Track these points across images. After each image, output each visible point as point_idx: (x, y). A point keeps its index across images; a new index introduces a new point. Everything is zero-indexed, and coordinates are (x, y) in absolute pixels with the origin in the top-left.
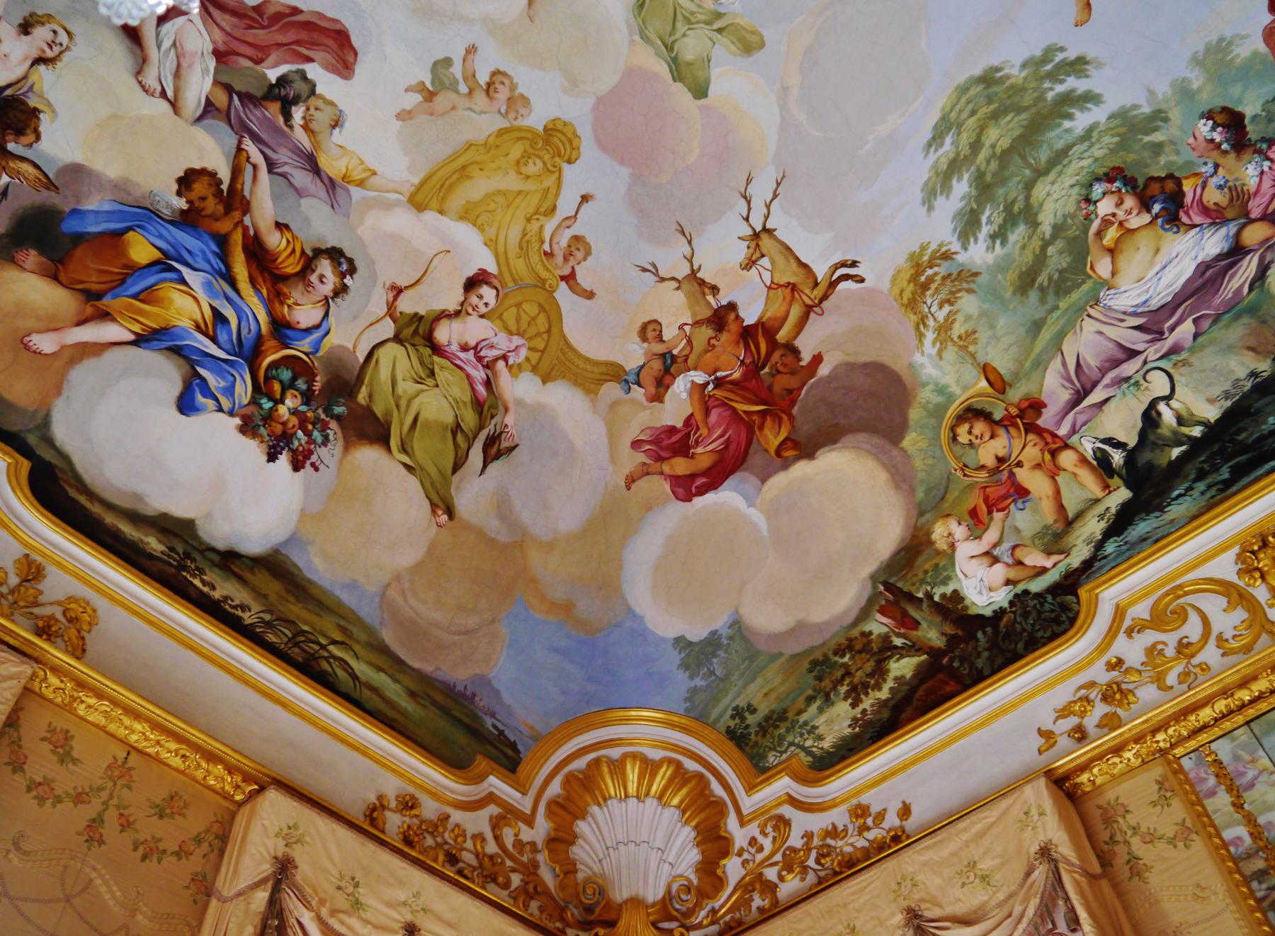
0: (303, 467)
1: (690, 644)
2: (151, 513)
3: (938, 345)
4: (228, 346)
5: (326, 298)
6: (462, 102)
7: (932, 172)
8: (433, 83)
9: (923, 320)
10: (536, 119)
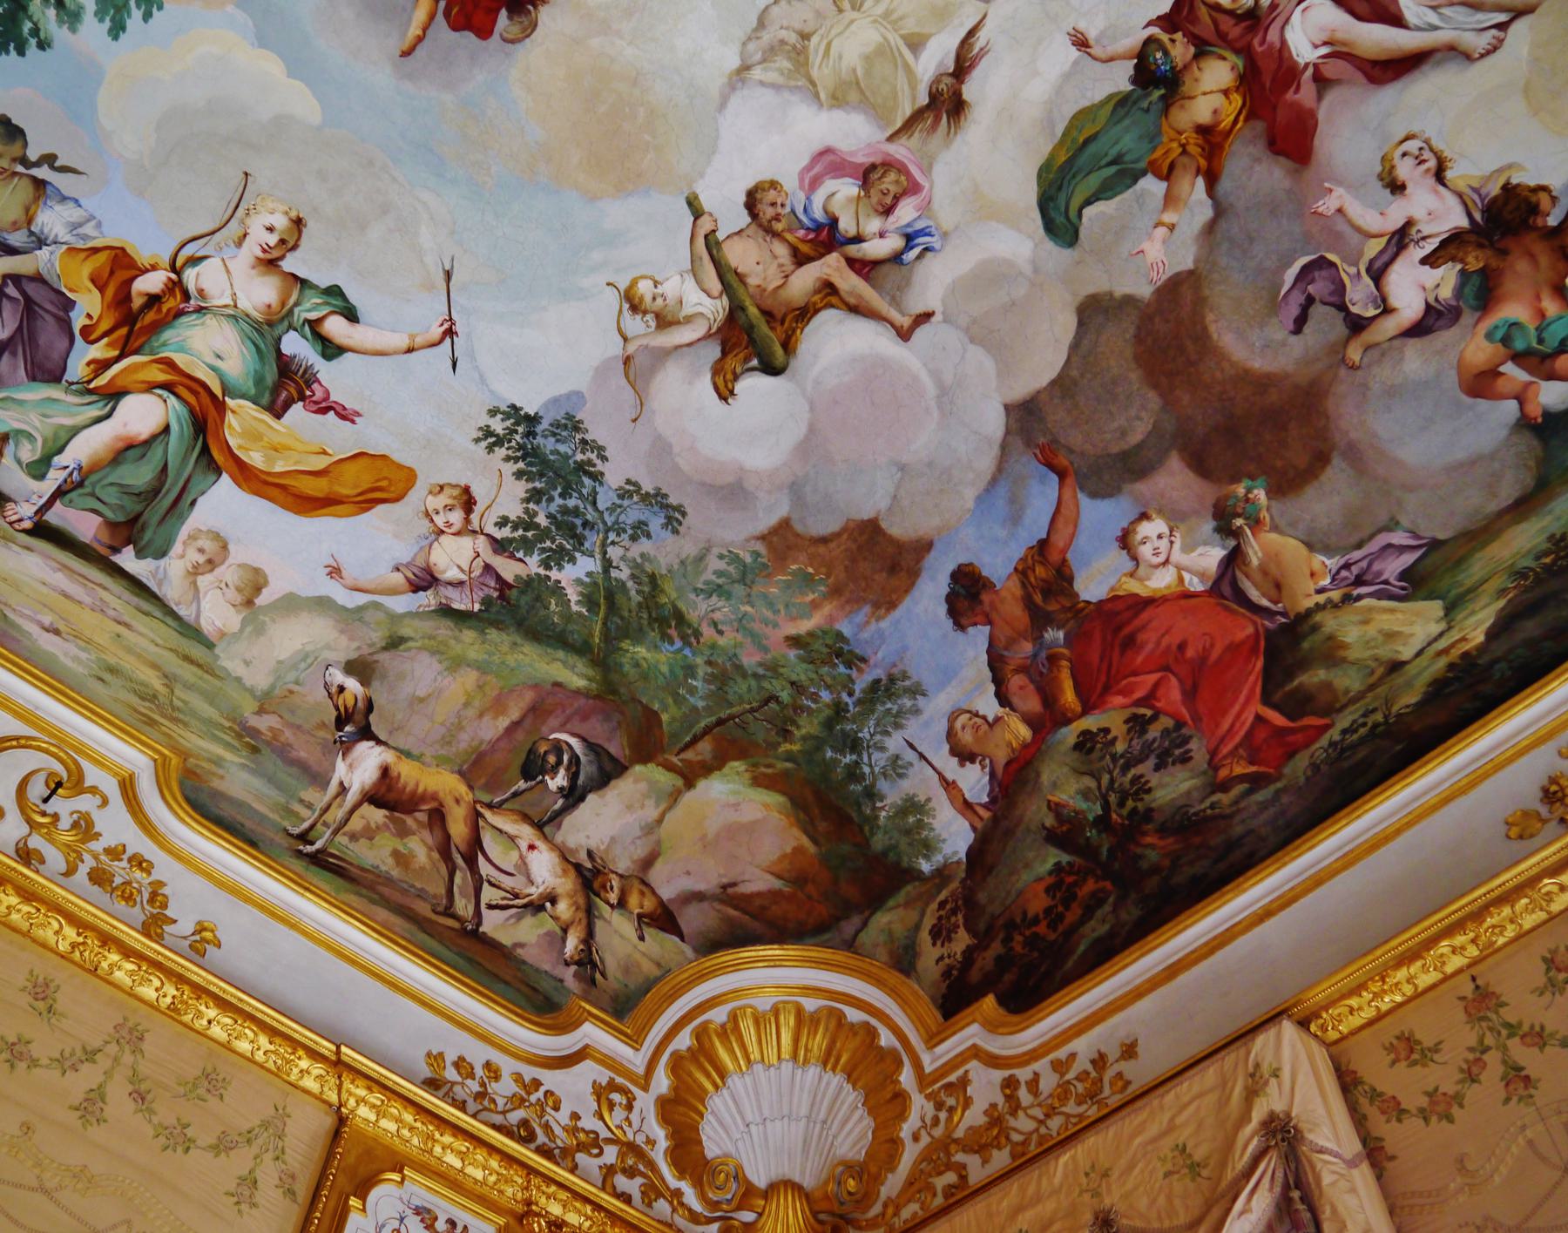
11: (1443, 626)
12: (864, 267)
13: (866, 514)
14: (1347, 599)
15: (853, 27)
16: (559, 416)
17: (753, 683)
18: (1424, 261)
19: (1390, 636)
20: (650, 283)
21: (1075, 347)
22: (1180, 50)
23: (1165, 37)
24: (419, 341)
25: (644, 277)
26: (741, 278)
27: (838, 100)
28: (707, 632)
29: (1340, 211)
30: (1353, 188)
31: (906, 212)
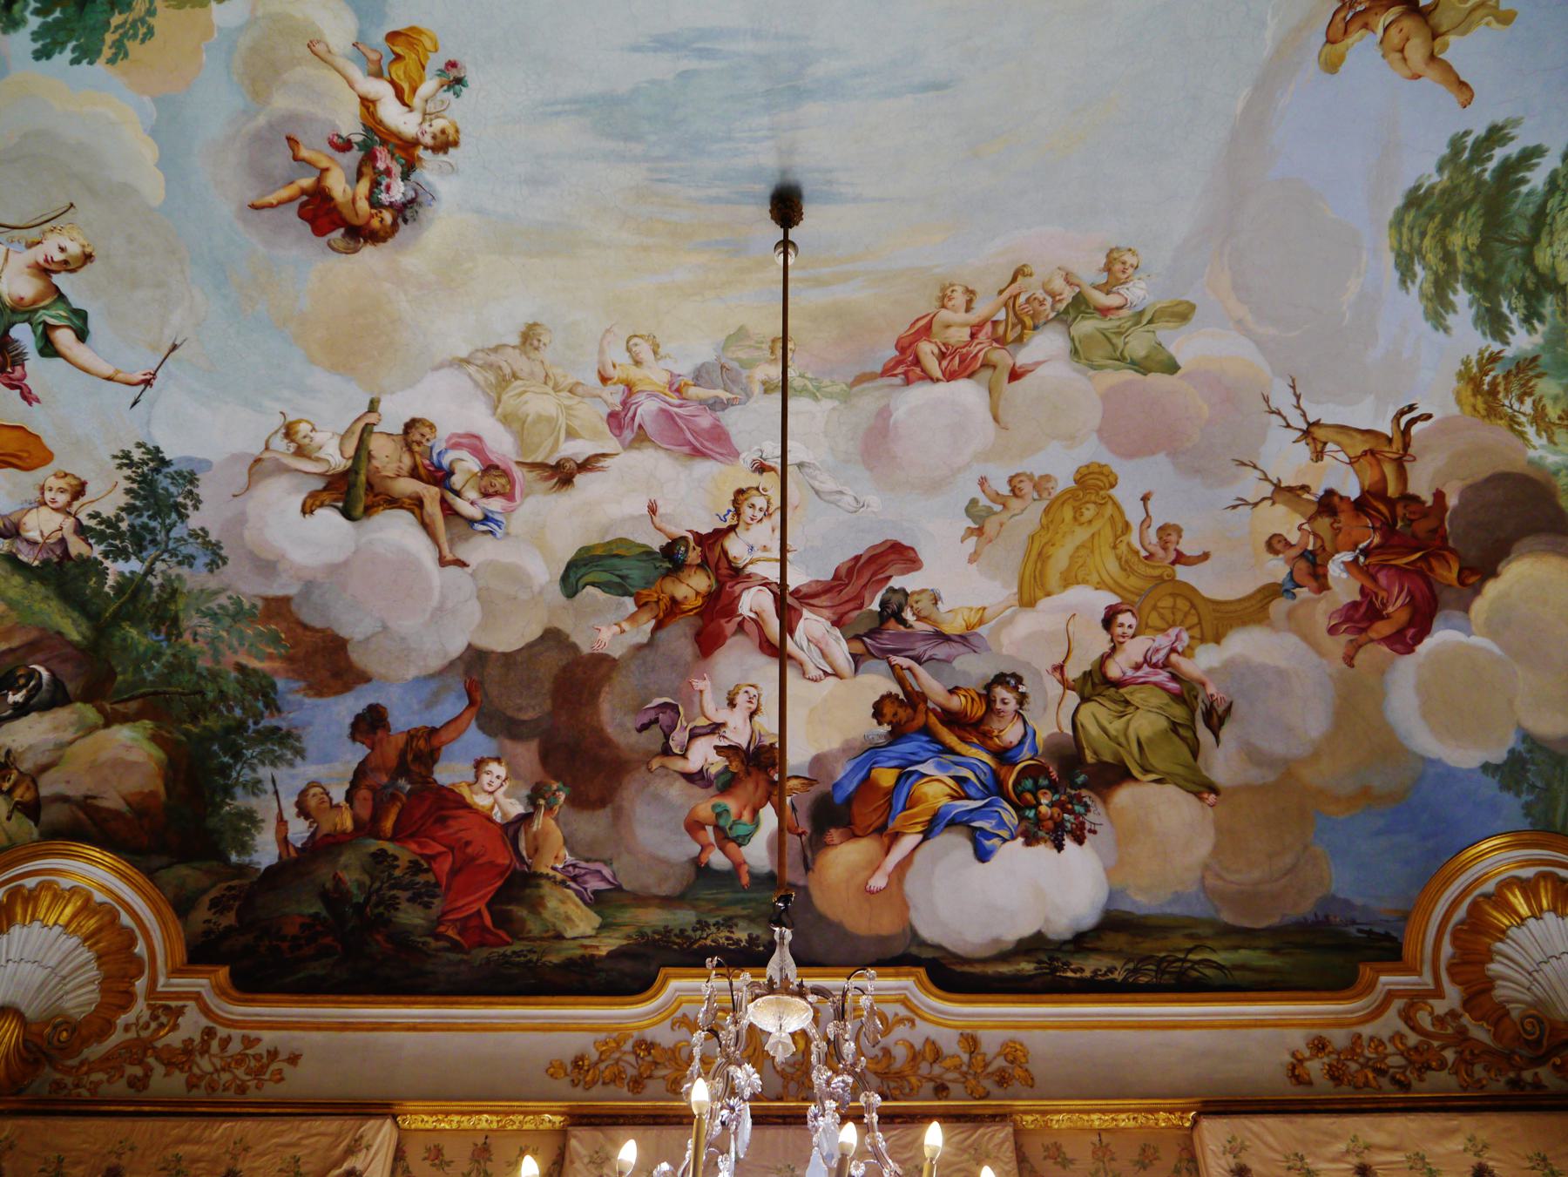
0: (1085, 837)
1: (1497, 767)
2: (1011, 947)
3: (1544, 434)
4: (979, 795)
5: (1016, 711)
6: (1004, 517)
7: (1424, 302)
8: (975, 522)
9: (1512, 422)
10: (1064, 480)
11: (593, 933)
12: (449, 510)
13: (344, 633)
14: (563, 883)
15: (545, 397)
16: (185, 468)
17: (194, 677)
18: (716, 747)
19: (568, 919)
20: (310, 427)
21: (530, 646)
22: (694, 556)
23: (692, 544)
24: (121, 376)
25: (308, 422)
26: (370, 457)
27: (506, 420)
28: (187, 637)
29: (701, 692)
30: (715, 688)
31: (495, 505)
